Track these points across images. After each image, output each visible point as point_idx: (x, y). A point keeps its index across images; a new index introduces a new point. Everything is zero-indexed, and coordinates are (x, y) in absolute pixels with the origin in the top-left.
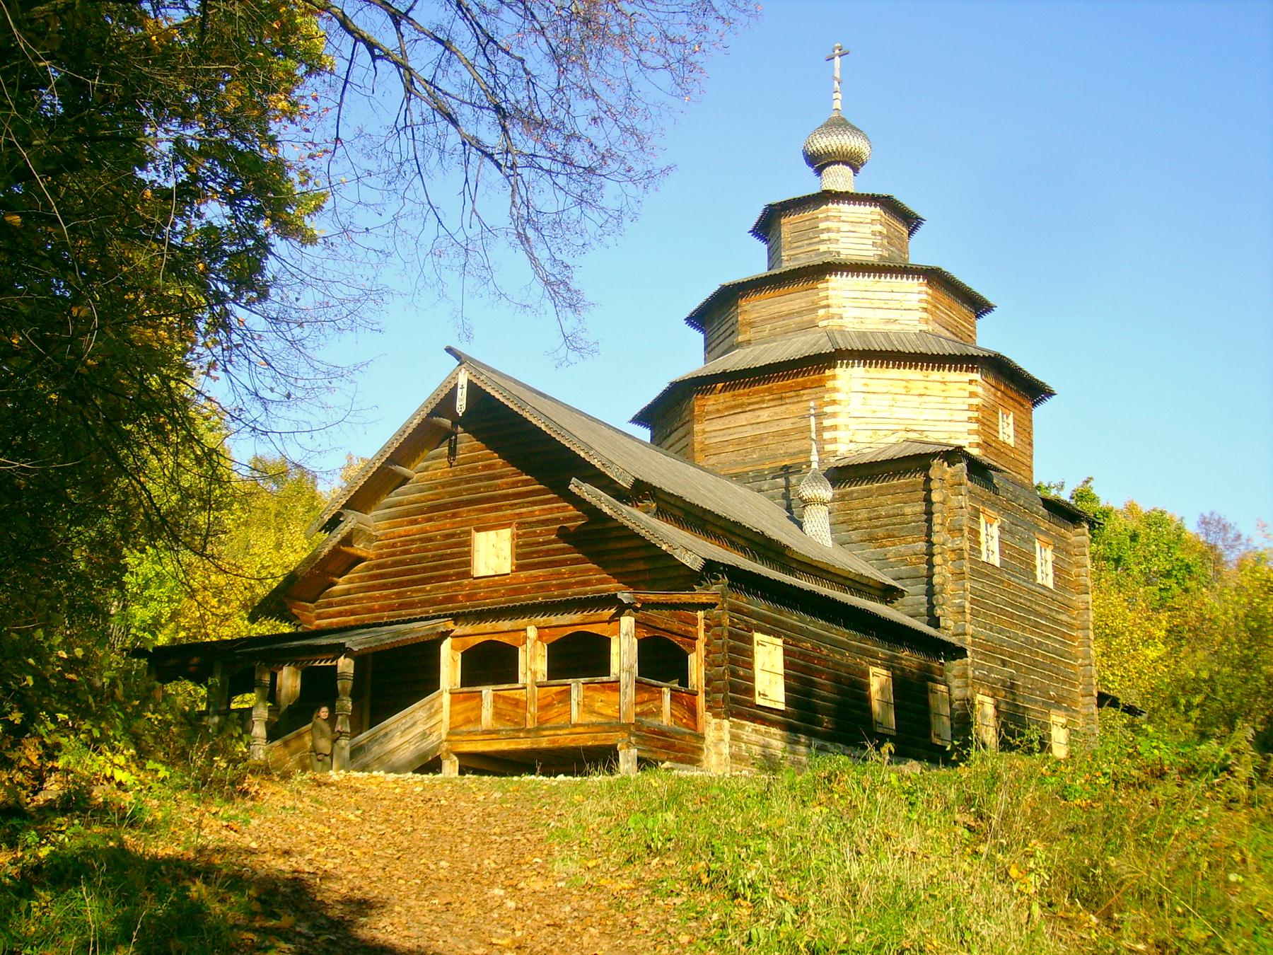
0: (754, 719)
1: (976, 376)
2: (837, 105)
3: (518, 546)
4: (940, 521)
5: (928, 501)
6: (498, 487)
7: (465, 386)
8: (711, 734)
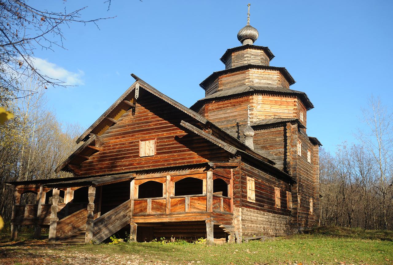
1: (296, 100)
2: (249, 21)
3: (157, 146)
4: (289, 142)
5: (285, 136)
6: (150, 126)
7: (138, 89)
8: (235, 213)
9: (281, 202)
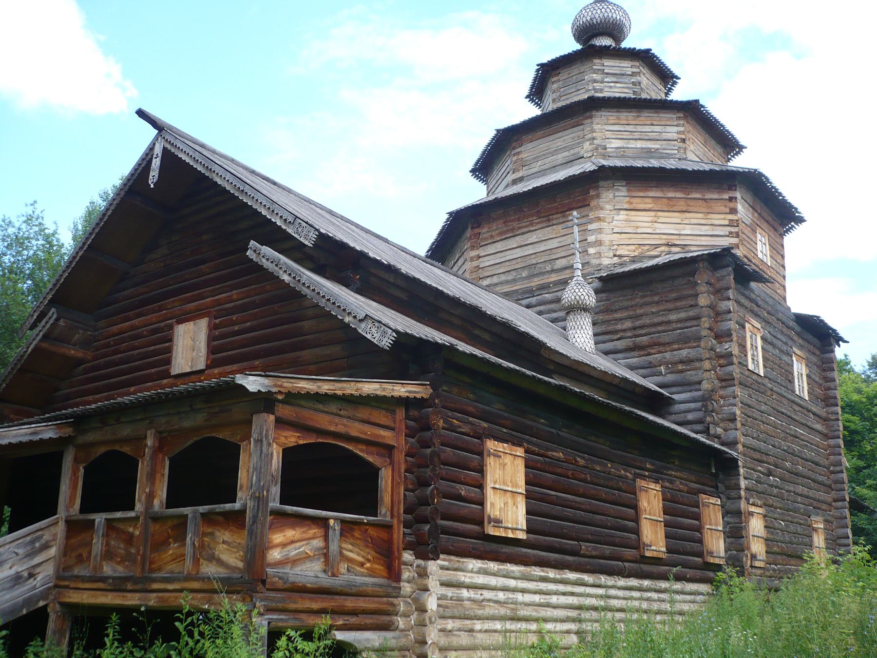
7: (160, 155)
9: (666, 532)
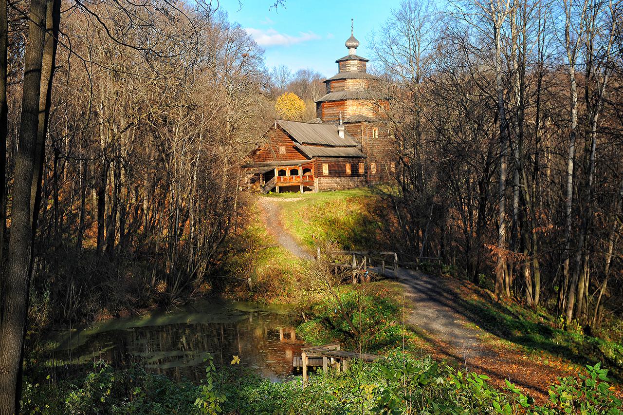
0: (323, 177)
8: (315, 181)
